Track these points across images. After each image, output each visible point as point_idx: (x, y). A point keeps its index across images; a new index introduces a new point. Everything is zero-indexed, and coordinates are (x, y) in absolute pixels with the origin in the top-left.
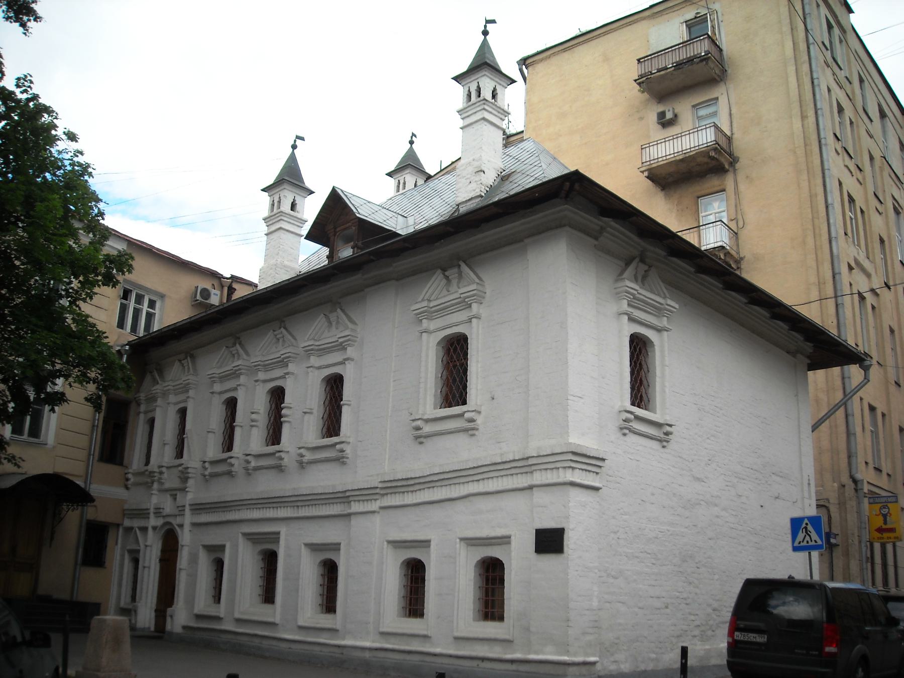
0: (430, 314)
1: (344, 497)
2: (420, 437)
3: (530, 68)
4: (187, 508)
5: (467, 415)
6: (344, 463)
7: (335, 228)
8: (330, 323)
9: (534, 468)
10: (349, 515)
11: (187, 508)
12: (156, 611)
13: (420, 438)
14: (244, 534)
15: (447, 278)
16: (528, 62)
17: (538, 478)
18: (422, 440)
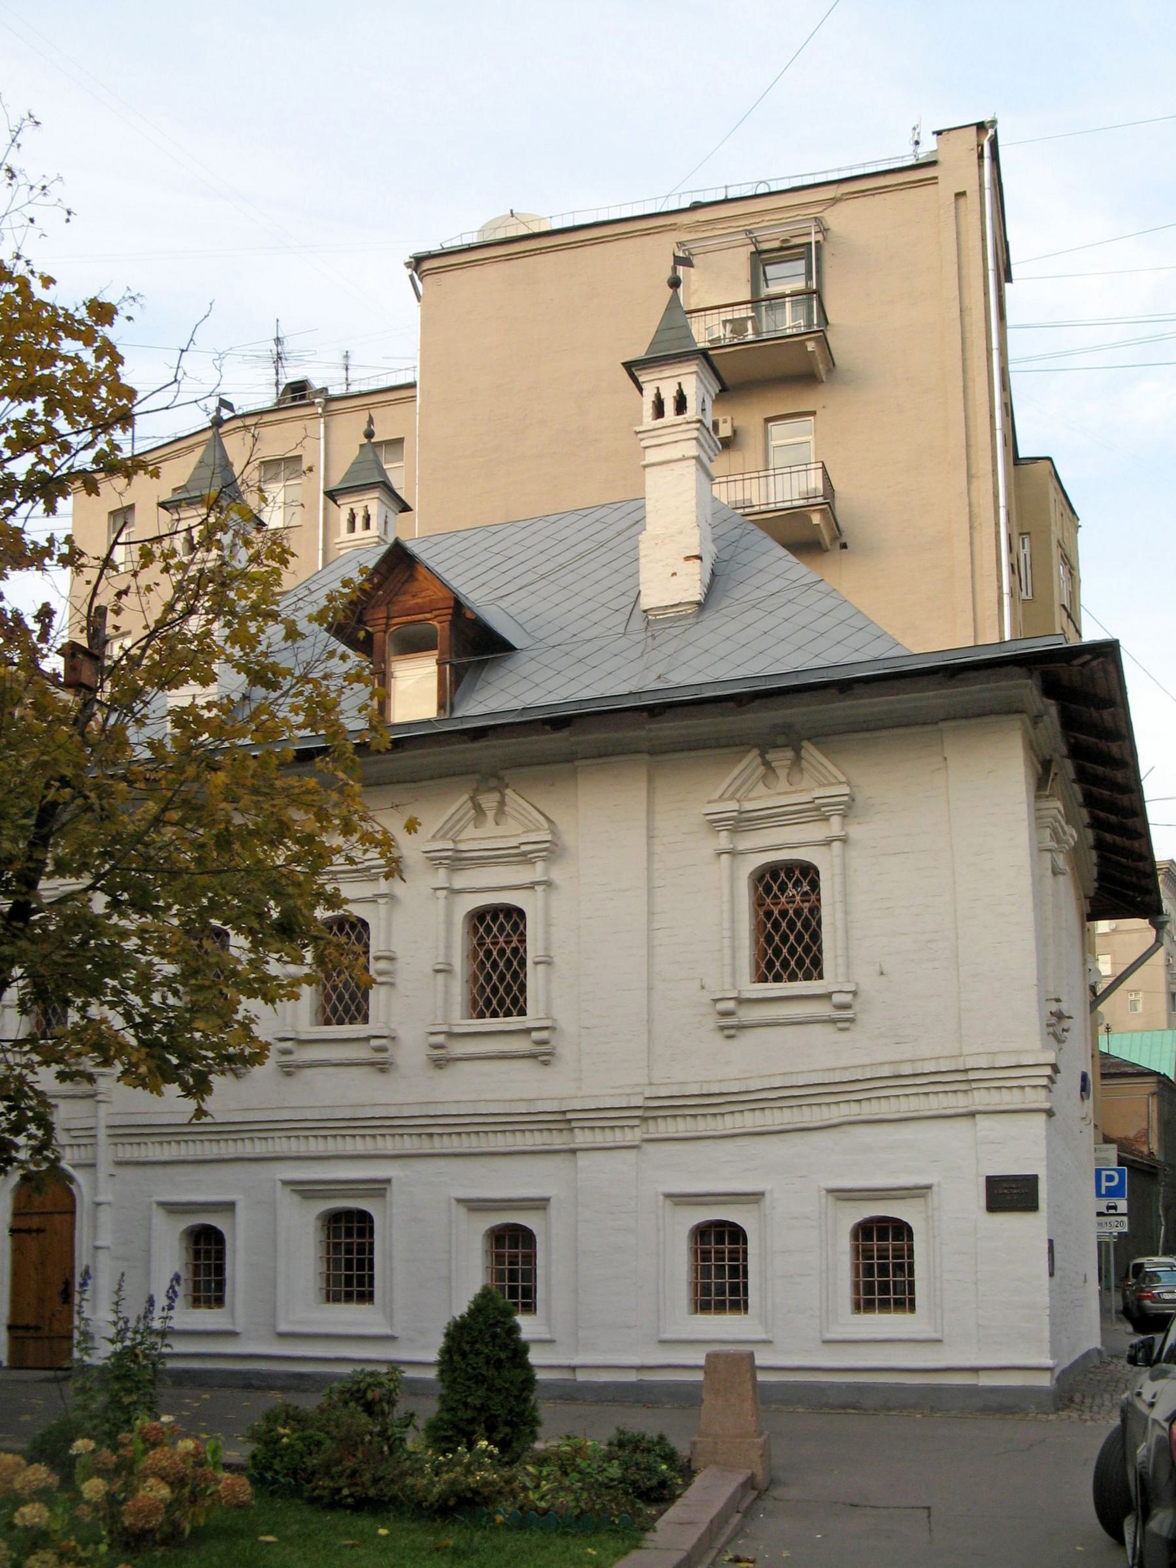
0: (741, 823)
1: (564, 1120)
2: (732, 1027)
3: (428, 279)
4: (102, 1133)
5: (837, 998)
6: (546, 1063)
7: (388, 618)
8: (478, 807)
9: (974, 1085)
10: (573, 1151)
11: (102, 1133)
12: (11, 1328)
13: (731, 1029)
14: (286, 1183)
15: (767, 764)
16: (426, 265)
17: (980, 1099)
18: (732, 1032)
